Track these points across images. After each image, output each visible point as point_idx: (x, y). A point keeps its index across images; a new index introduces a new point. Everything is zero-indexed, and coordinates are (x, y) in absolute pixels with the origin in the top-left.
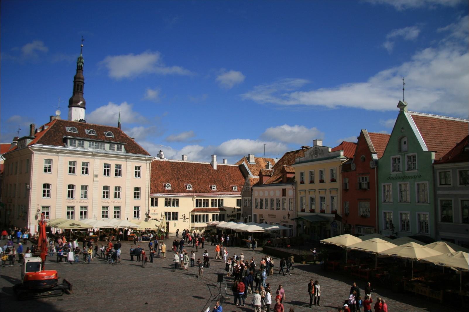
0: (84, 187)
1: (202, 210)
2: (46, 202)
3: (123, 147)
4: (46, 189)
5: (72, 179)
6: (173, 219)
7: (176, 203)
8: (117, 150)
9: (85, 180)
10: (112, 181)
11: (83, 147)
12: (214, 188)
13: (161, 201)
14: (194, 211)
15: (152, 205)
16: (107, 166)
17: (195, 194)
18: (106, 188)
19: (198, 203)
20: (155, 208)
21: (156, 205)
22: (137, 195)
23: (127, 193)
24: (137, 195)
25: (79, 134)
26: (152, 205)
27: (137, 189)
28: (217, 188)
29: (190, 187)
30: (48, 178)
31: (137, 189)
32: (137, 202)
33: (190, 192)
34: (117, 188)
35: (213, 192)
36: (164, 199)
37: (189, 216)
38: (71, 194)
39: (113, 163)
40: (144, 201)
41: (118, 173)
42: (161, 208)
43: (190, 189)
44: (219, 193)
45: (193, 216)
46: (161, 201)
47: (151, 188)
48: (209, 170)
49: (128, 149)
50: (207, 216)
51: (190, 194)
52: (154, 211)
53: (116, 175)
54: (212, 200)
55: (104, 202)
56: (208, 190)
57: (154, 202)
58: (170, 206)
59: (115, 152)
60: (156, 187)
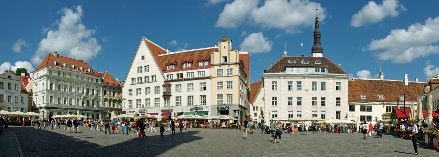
8: (322, 72)
10: (319, 94)
13: (357, 108)
16: (315, 83)
18: (314, 98)
20: (352, 112)
21: (354, 110)
23: (331, 102)
27: (338, 99)
31: (338, 99)
32: (338, 109)
36: (360, 106)
39: (319, 81)
40: (344, 108)
46: (357, 108)
53: (322, 89)
57: (352, 108)
59: (320, 73)
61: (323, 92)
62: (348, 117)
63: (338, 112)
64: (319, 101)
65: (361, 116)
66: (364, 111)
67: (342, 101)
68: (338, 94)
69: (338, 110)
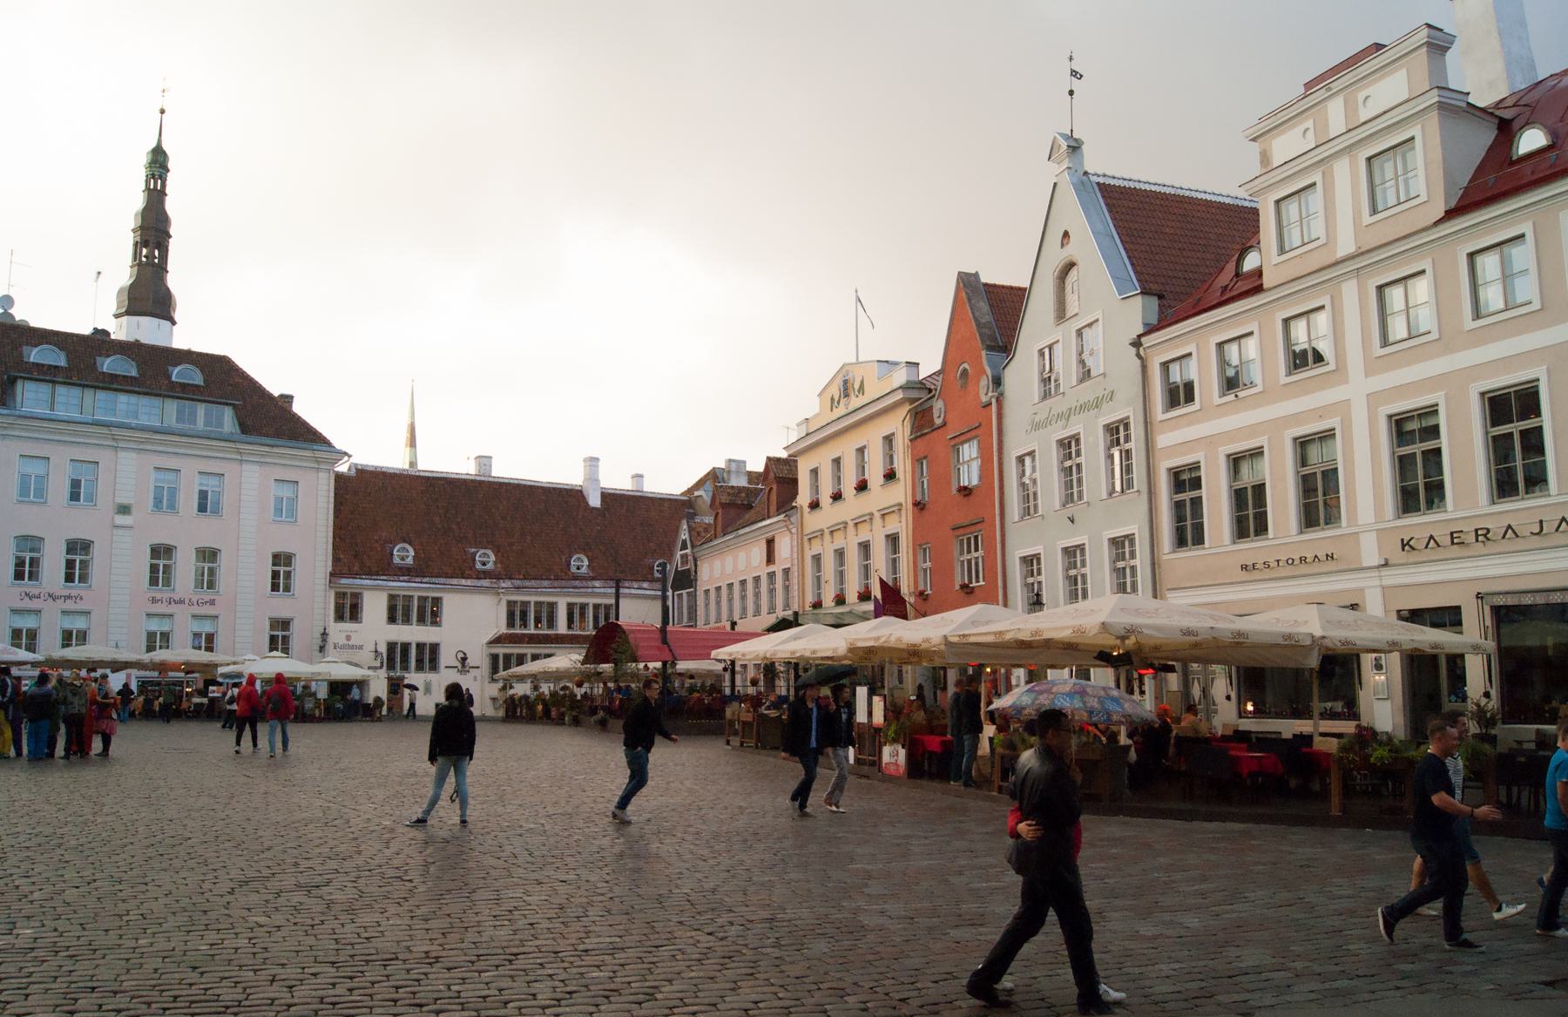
0: (78, 547)
5: (31, 521)
6: (420, 667)
7: (430, 613)
9: (80, 523)
10: (187, 532)
12: (580, 563)
13: (375, 604)
14: (498, 640)
15: (340, 617)
17: (507, 584)
18: (161, 552)
19: (516, 614)
20: (348, 626)
22: (280, 581)
23: (245, 574)
24: (280, 581)
26: (340, 617)
29: (486, 558)
32: (281, 606)
33: (486, 575)
35: (575, 578)
38: (25, 569)
42: (375, 628)
43: (490, 566)
44: (597, 584)
45: (495, 658)
46: (375, 604)
47: (336, 560)
51: (486, 583)
52: (348, 638)
54: (570, 607)
55: (154, 601)
56: (561, 575)
62: (330, 647)
65: (391, 647)
66: (407, 620)
67: (299, 568)
69: (284, 614)
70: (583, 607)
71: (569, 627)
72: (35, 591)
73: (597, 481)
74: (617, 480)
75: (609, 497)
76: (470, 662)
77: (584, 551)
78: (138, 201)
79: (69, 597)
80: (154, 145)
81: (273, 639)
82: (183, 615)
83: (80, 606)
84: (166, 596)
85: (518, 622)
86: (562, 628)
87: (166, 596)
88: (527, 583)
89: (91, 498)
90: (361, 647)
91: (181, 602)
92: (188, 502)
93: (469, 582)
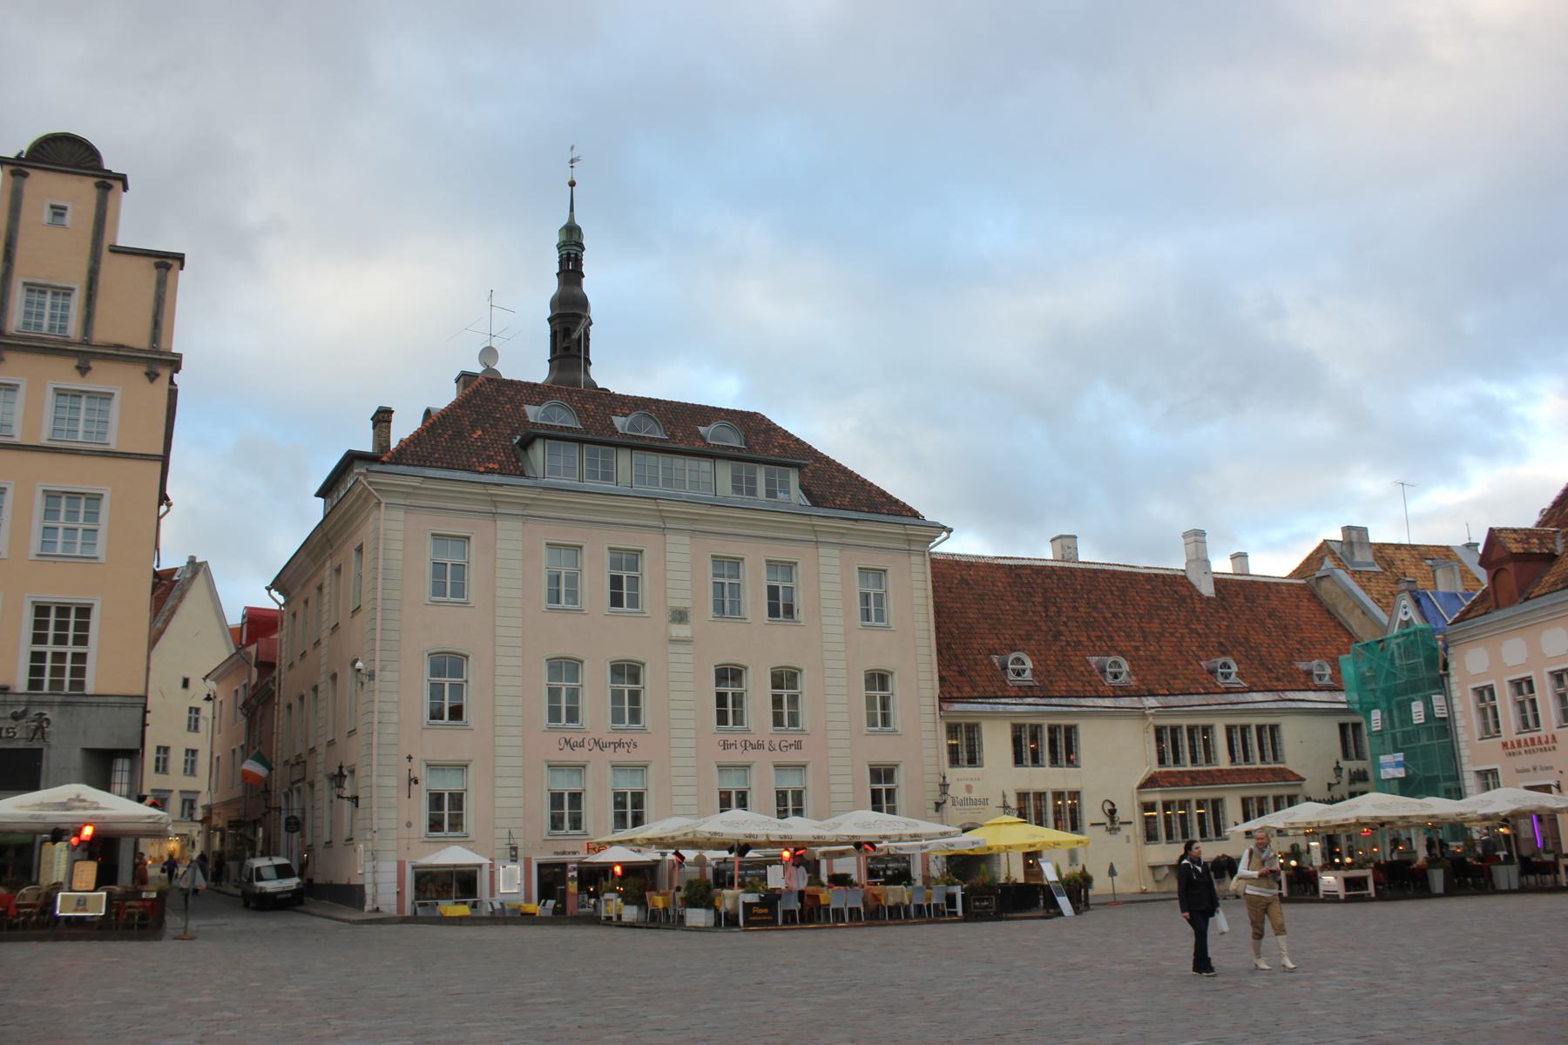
0: (627, 671)
1: (1195, 778)
2: (446, 742)
3: (794, 478)
4: (447, 681)
5: (563, 634)
7: (1063, 746)
9: (626, 636)
10: (759, 646)
11: (607, 477)
13: (996, 741)
14: (1150, 782)
15: (954, 761)
18: (729, 674)
20: (966, 772)
21: (973, 761)
22: (880, 714)
23: (833, 702)
24: (880, 714)
25: (587, 430)
26: (954, 761)
27: (878, 679)
28: (1239, 674)
30: (447, 628)
32: (882, 750)
34: (784, 678)
35: (1228, 691)
37: (1129, 810)
38: (563, 709)
41: (780, 607)
46: (996, 741)
47: (942, 679)
48: (1183, 599)
49: (815, 490)
50: (1217, 805)
52: (969, 789)
55: (726, 745)
57: (964, 747)
58: (1036, 761)
60: (964, 669)
61: (781, 630)
63: (882, 774)
64: (757, 693)
65: (1022, 796)
68: (879, 651)
70: (1245, 729)
71: (1233, 760)
72: (577, 738)
73: (1207, 562)
74: (1221, 565)
75: (1221, 583)
76: (1121, 815)
77: (1224, 654)
78: (552, 286)
79: (620, 744)
80: (565, 221)
81: (876, 795)
82: (762, 762)
83: (635, 756)
84: (740, 738)
85: (1170, 756)
86: (1223, 762)
87: (740, 738)
88: (1172, 700)
89: (634, 602)
90: (985, 802)
91: (760, 746)
92: (754, 600)
93: (1108, 702)
